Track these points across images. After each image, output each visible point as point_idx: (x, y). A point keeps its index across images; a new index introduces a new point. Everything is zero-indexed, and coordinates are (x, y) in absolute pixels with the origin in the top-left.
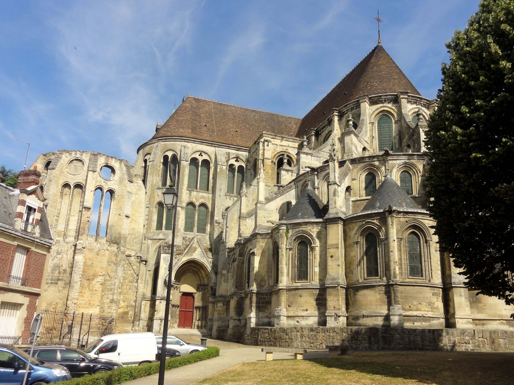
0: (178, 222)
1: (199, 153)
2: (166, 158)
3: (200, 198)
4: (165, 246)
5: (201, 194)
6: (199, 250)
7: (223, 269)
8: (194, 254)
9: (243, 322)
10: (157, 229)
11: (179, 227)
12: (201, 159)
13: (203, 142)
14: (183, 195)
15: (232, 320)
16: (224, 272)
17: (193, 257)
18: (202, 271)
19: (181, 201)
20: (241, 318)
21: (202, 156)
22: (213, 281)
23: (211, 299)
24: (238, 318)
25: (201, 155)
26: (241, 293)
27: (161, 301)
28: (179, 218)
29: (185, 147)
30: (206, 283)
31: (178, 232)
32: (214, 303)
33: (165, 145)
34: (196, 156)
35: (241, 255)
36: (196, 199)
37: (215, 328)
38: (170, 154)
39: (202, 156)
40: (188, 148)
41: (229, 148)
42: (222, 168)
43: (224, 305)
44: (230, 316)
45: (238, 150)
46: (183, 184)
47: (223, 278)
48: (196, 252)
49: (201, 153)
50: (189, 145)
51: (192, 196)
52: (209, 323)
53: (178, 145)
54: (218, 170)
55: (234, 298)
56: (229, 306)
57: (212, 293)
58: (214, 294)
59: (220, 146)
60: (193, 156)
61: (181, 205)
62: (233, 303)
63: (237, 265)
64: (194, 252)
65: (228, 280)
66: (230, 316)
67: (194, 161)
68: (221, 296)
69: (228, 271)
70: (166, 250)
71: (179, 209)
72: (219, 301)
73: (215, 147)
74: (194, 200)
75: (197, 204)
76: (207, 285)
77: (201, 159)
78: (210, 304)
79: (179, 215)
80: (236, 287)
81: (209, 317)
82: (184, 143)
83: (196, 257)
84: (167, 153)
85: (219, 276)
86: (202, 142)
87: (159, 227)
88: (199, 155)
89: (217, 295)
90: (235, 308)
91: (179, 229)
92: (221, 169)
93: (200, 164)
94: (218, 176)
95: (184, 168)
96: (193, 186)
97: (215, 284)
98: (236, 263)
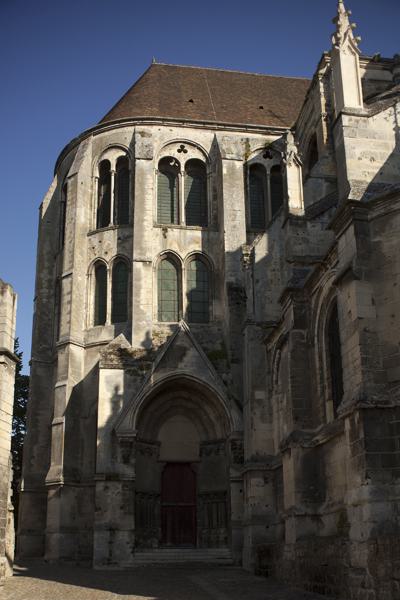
0: (138, 295)
1: (178, 146)
2: (104, 166)
3: (190, 243)
4: (110, 353)
5: (189, 233)
6: (191, 353)
7: (255, 387)
8: (181, 365)
9: (329, 523)
10: (96, 324)
11: (142, 307)
12: (183, 159)
13: (183, 122)
14: (146, 234)
15: (293, 519)
16: (260, 395)
17: (178, 371)
18: (208, 409)
19: (141, 249)
20: (321, 510)
21: (186, 152)
22: (234, 427)
23: (234, 473)
24: (310, 511)
25: (182, 150)
26: (314, 435)
27: (109, 484)
28: (140, 288)
29: (143, 134)
30: (219, 436)
31: (139, 320)
32: (239, 481)
33: (101, 139)
34: (173, 152)
35: (301, 322)
36: (179, 246)
37: (248, 543)
38: (113, 157)
39: (186, 152)
40: (150, 135)
41: (246, 129)
42: (234, 166)
43: (266, 482)
44: (287, 506)
45: (269, 134)
46: (143, 210)
47: (258, 412)
48: (185, 359)
49: (182, 147)
50: (154, 130)
51: (169, 239)
52: (233, 532)
53: (124, 134)
54: (225, 171)
55: (294, 452)
56: (281, 482)
57: (236, 458)
58: (240, 460)
59: (224, 127)
60: (166, 154)
61: (143, 258)
62: (290, 467)
63: (293, 351)
64: (181, 359)
65: (271, 415)
66: (287, 506)
67: (167, 167)
68: (254, 459)
69: (270, 391)
70: (112, 360)
71: (137, 266)
72: (251, 471)
73: (214, 129)
74: (175, 248)
75: (183, 255)
76: (223, 440)
77: (183, 159)
78: (232, 485)
79: (139, 280)
80: (296, 418)
81: (233, 517)
82: (139, 128)
83: (187, 371)
84: (106, 156)
85: (247, 408)
86: (181, 123)
87: (100, 319)
88: (179, 151)
89: (247, 457)
90: (298, 481)
91: (143, 313)
92: (232, 169)
93: (183, 169)
94: (225, 185)
95: (143, 174)
96: (168, 219)
97: (241, 433)
98: (287, 350)
